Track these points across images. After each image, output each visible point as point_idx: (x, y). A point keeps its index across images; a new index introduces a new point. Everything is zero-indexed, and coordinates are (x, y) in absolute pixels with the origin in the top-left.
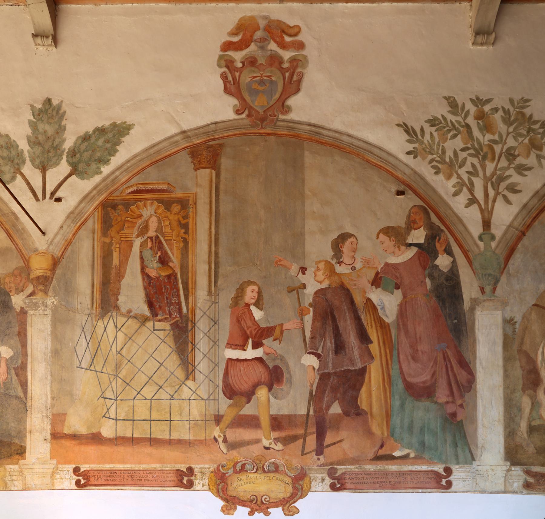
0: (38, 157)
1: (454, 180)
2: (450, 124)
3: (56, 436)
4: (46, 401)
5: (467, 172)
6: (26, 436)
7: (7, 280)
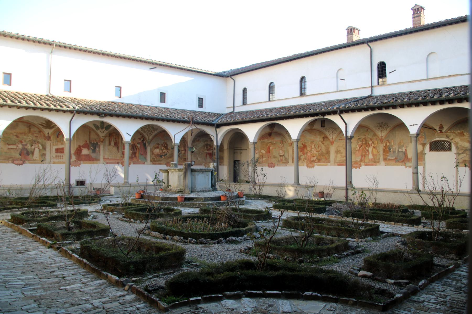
3: (104, 158)
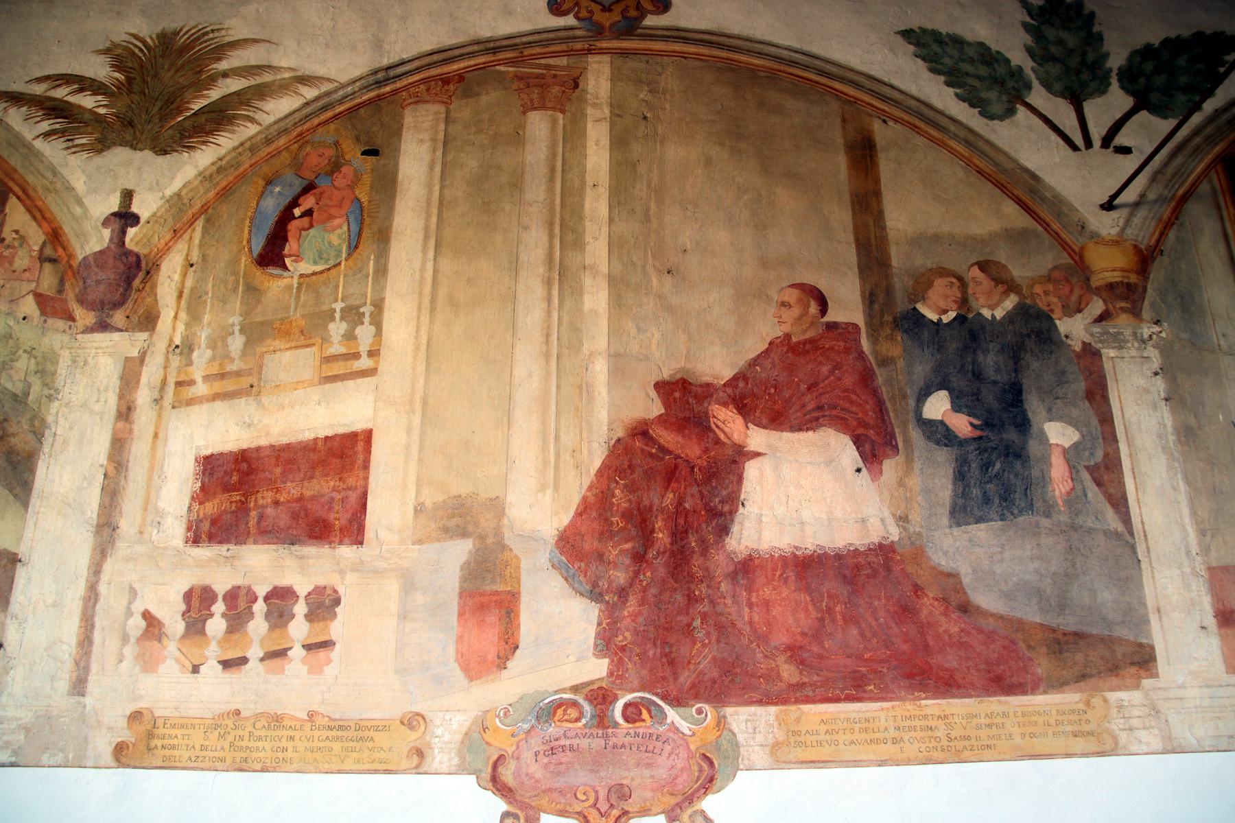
0: (1058, 79)
4: (1185, 538)
6: (1148, 622)
7: (1038, 289)
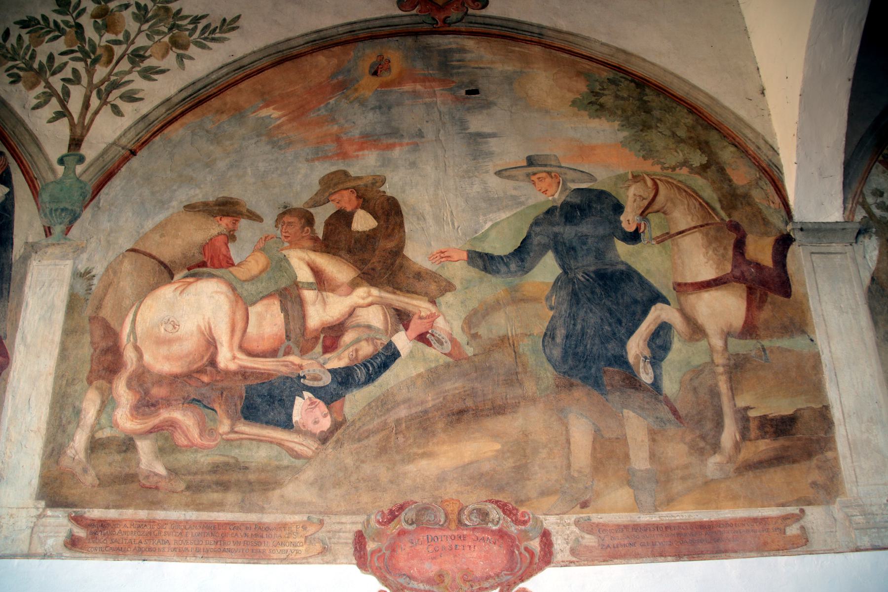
1: (40, 89)
2: (52, 25)
5: (63, 80)
